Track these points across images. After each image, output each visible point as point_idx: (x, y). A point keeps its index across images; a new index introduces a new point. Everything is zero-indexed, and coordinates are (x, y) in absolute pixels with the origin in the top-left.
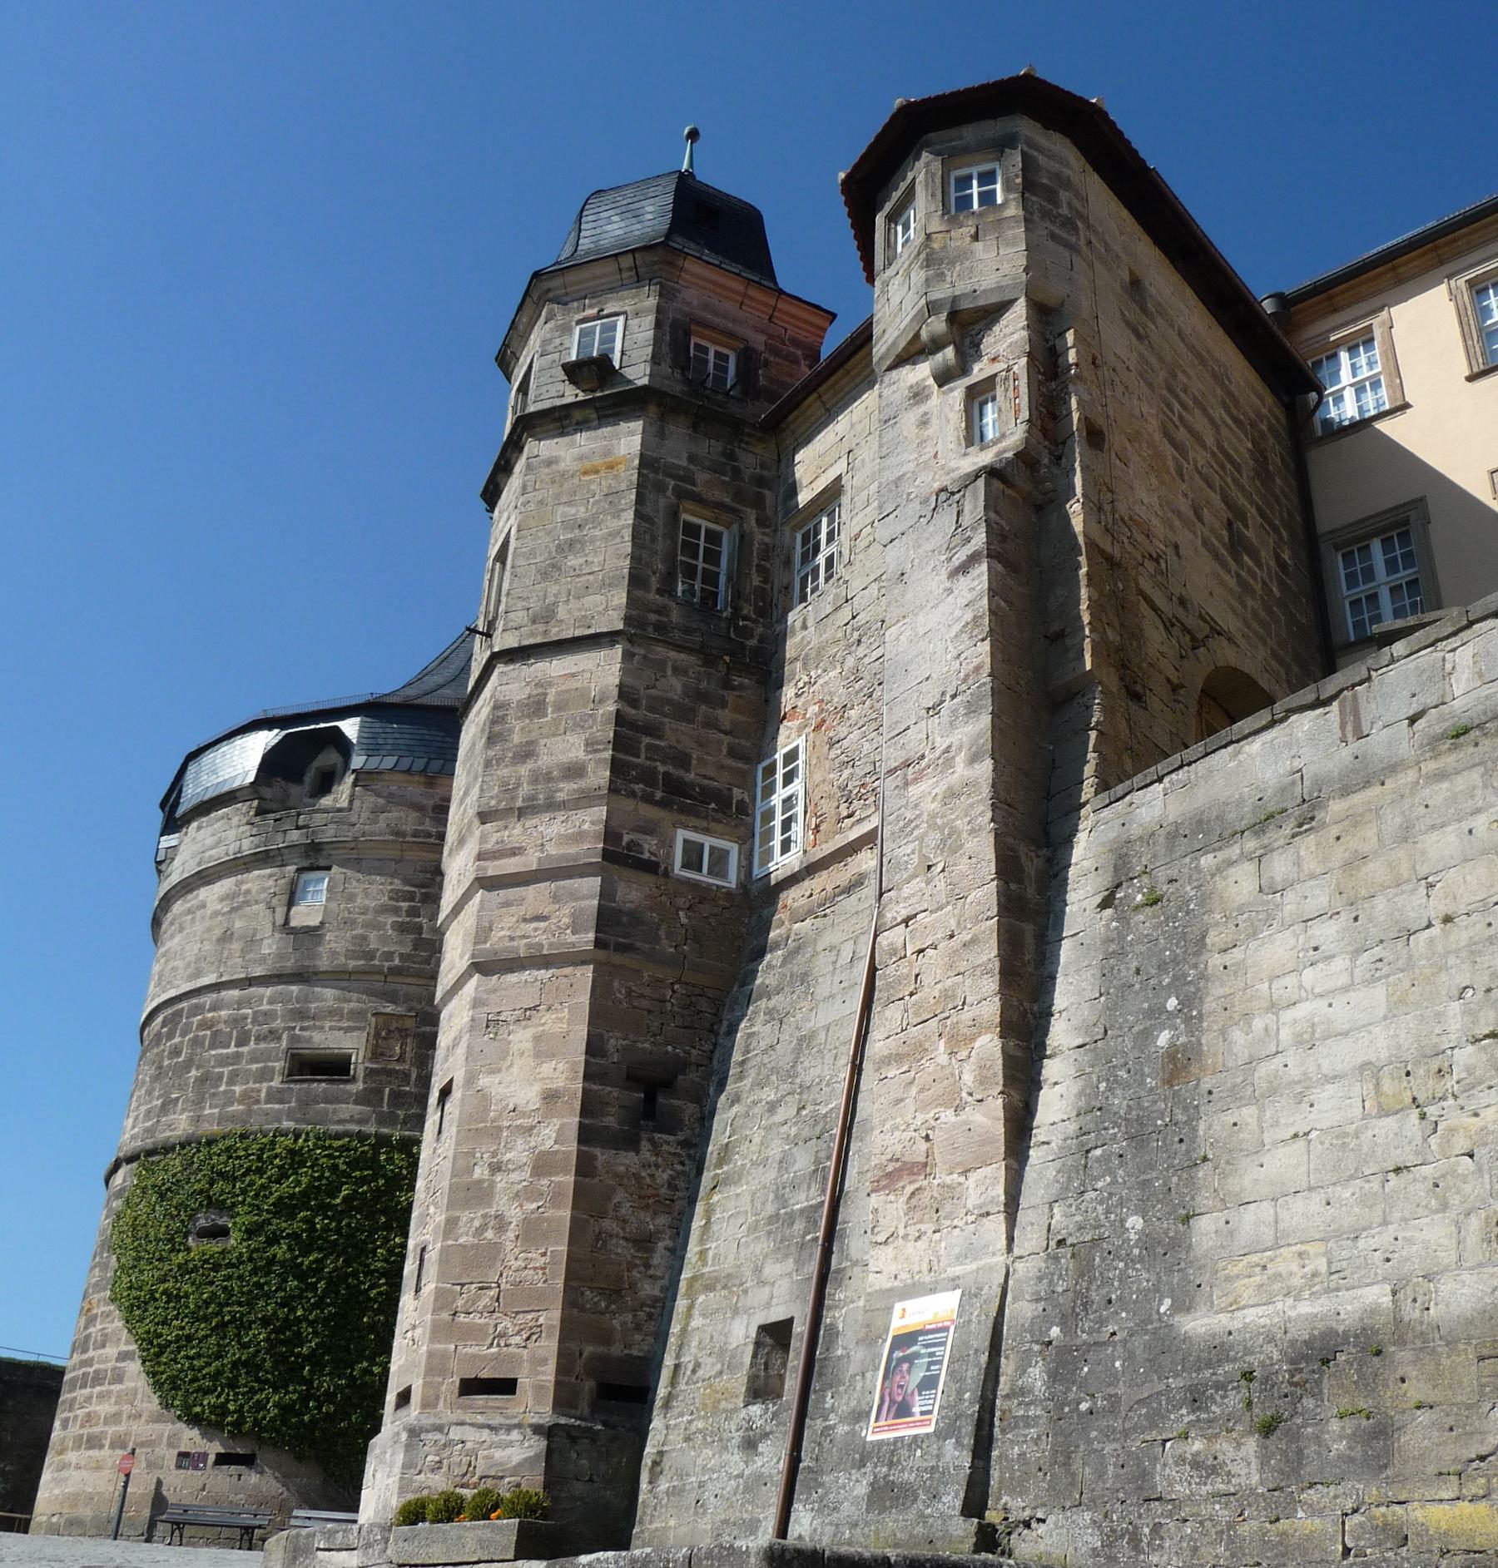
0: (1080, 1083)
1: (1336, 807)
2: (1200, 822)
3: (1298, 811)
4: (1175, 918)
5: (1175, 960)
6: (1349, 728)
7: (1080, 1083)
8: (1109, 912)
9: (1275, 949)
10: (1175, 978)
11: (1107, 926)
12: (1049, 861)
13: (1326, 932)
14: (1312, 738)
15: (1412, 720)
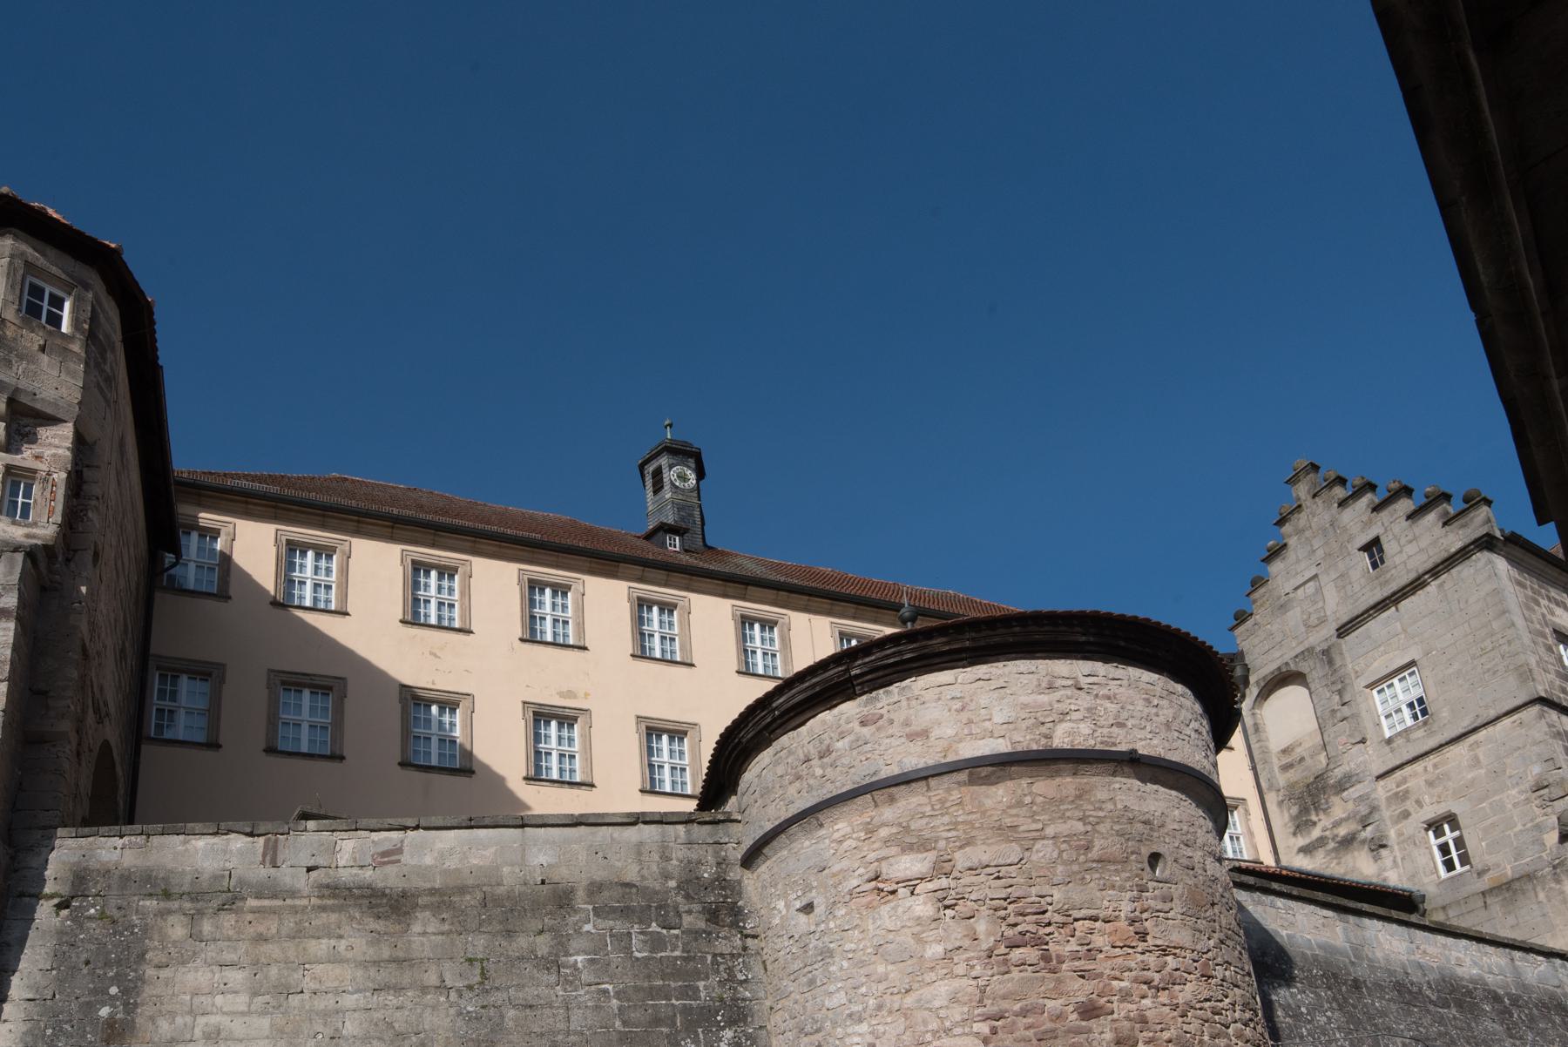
0: (29, 1025)
1: (252, 902)
2: (150, 877)
3: (227, 896)
4: (121, 934)
5: (119, 962)
6: (268, 858)
7: (29, 1025)
8: (65, 912)
9: (197, 976)
10: (117, 974)
11: (62, 922)
12: (13, 858)
13: (236, 977)
14: (240, 852)
15: (309, 869)
